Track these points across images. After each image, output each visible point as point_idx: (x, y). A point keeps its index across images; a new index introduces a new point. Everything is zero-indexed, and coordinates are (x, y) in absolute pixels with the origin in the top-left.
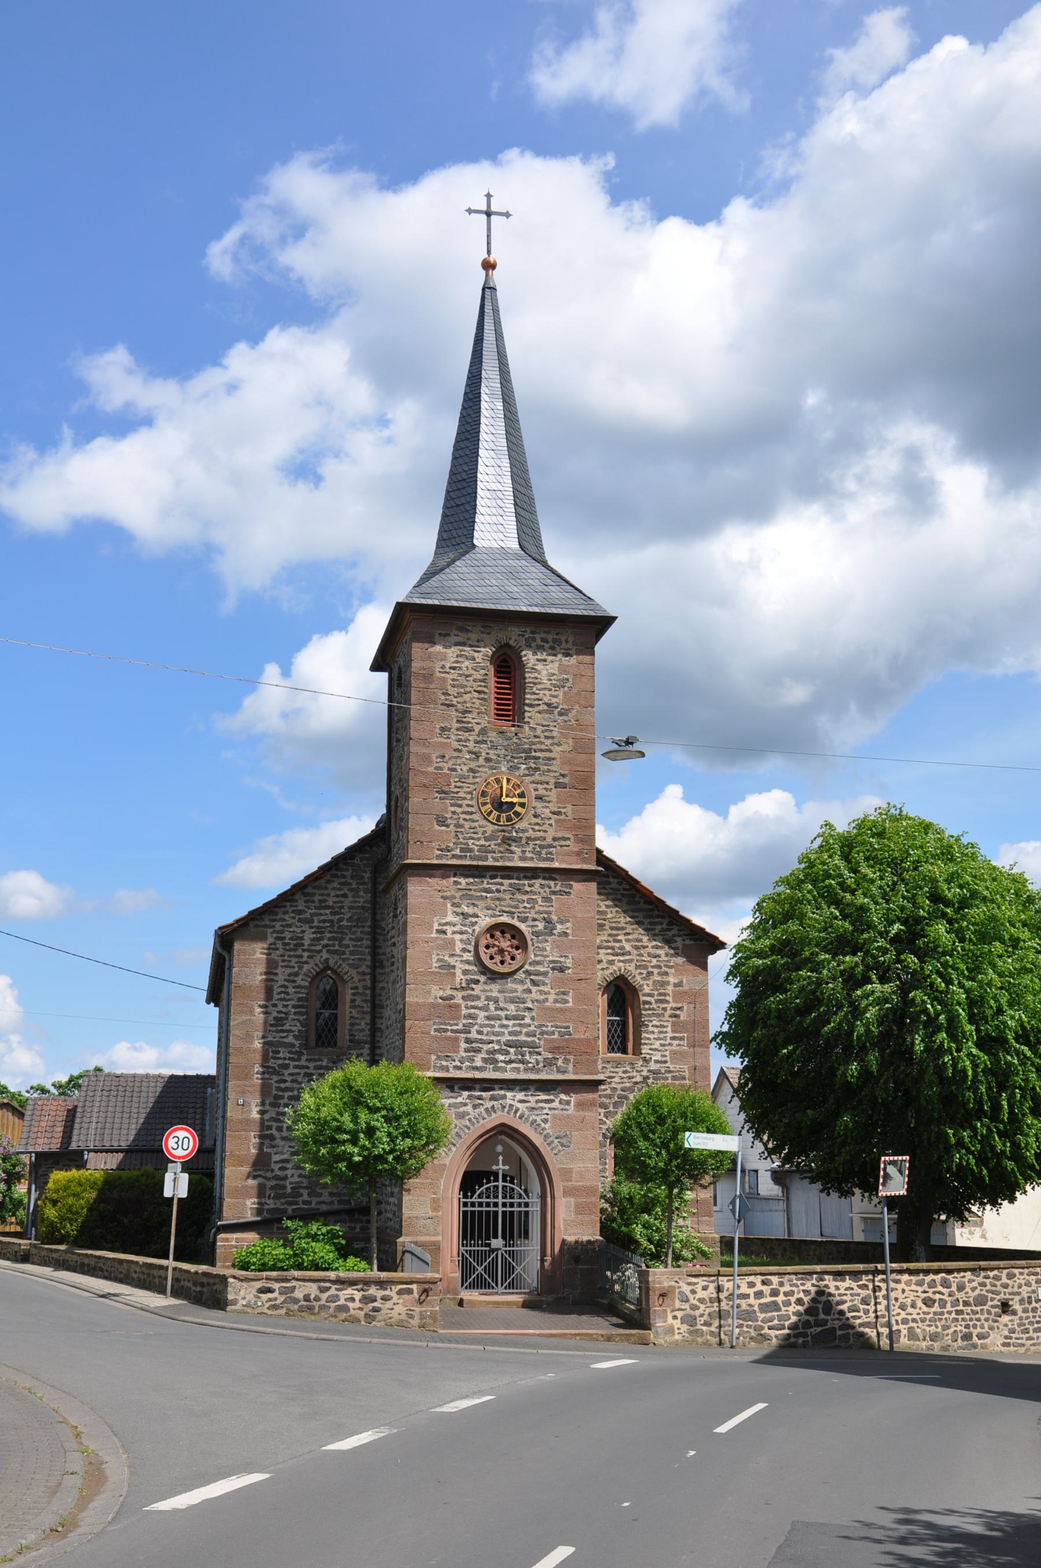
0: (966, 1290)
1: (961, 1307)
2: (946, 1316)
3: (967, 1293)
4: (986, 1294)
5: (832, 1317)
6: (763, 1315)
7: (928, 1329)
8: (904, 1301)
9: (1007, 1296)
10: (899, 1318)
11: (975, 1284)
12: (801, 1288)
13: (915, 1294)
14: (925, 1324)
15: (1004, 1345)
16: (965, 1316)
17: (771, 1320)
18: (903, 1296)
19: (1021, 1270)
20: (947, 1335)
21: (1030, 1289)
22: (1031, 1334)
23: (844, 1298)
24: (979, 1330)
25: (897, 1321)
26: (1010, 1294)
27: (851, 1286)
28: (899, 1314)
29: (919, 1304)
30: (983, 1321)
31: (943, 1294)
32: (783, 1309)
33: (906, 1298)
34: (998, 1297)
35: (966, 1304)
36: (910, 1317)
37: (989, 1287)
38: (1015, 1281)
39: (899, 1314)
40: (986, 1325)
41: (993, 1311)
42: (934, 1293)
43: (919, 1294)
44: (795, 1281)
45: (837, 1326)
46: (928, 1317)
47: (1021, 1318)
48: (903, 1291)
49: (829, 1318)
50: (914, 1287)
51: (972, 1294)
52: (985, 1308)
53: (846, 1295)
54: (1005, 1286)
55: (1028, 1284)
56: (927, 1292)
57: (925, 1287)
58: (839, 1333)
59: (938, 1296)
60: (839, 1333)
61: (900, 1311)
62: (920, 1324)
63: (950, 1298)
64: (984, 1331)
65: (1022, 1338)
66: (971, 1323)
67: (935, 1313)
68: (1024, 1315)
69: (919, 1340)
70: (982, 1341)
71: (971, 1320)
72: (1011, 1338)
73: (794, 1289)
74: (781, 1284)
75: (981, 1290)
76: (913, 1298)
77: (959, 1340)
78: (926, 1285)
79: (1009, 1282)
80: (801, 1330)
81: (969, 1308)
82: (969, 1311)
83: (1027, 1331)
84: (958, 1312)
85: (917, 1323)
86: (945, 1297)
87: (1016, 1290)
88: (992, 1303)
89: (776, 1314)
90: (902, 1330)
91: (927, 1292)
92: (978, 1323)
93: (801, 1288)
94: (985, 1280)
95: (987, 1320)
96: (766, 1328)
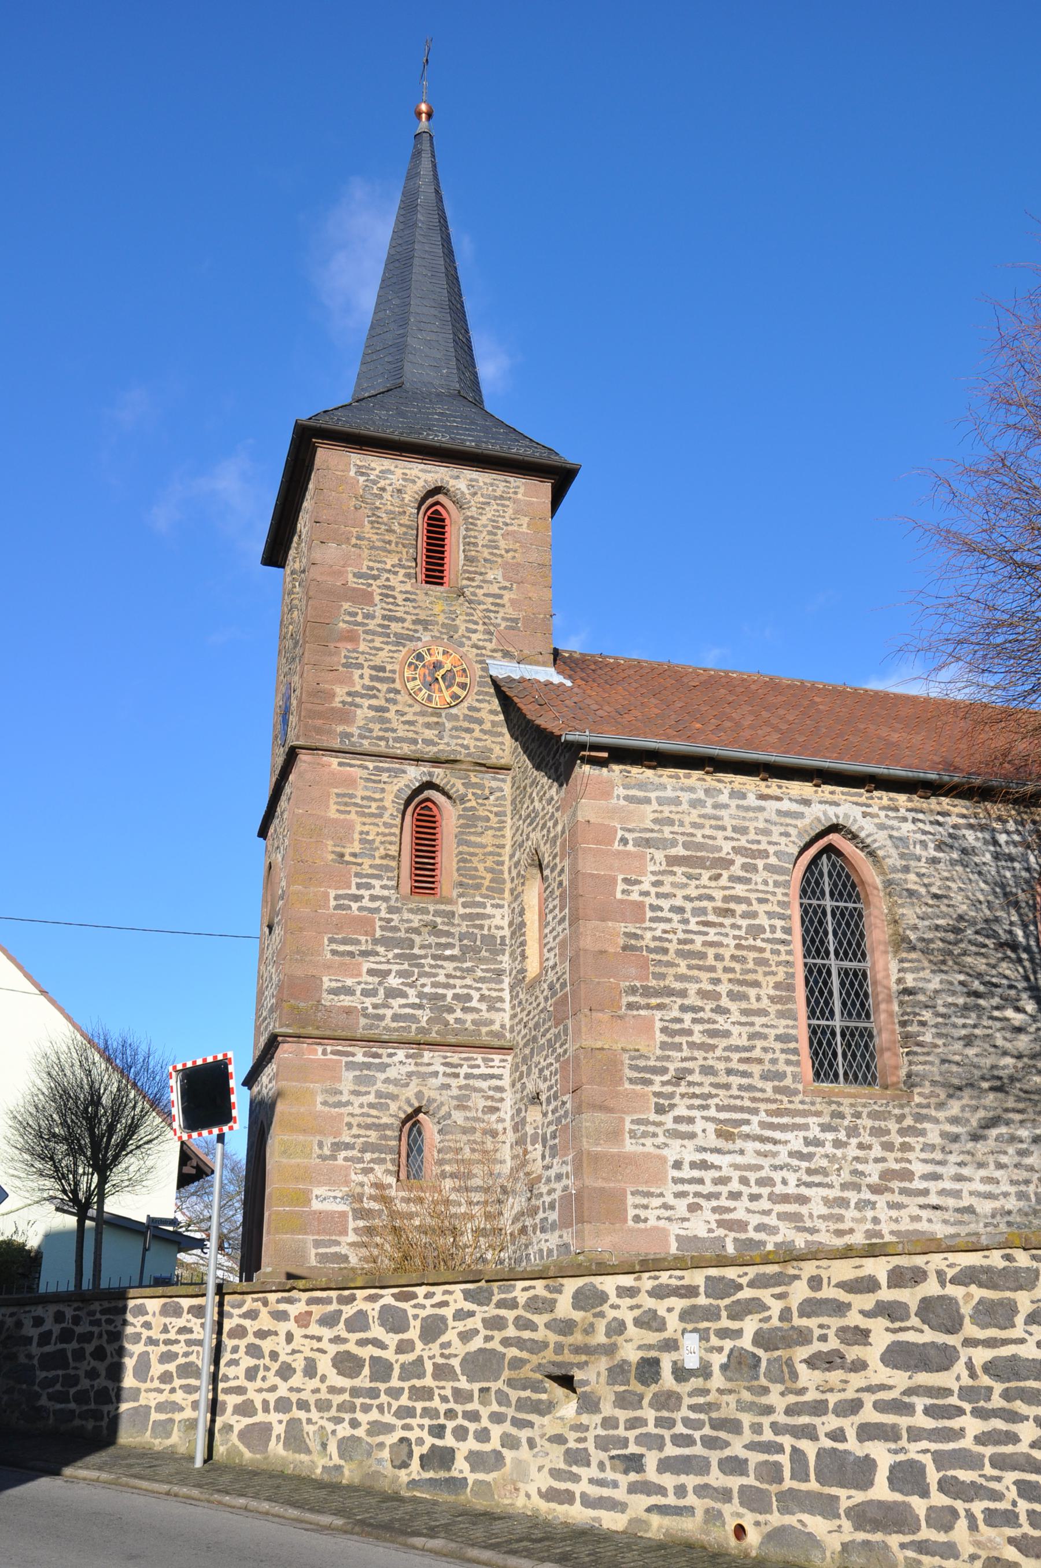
0: (444, 1339)
1: (428, 1381)
2: (384, 1398)
3: (447, 1345)
4: (501, 1349)
5: (148, 1385)
6: (44, 1374)
7: (330, 1426)
8: (289, 1359)
9: (568, 1357)
10: (272, 1397)
11: (470, 1323)
12: (105, 1327)
13: (316, 1345)
14: (326, 1415)
15: (551, 1495)
16: (436, 1403)
17: (54, 1381)
18: (289, 1349)
19: (627, 1281)
20: (381, 1445)
21: (652, 1337)
22: (651, 1474)
23: (174, 1348)
24: (471, 1444)
25: (266, 1403)
26: (577, 1350)
27: (189, 1325)
28: (273, 1389)
29: (325, 1365)
30: (485, 1422)
31: (382, 1346)
32: (72, 1364)
33: (294, 1352)
34: (535, 1359)
35: (442, 1372)
36: (294, 1397)
37: (511, 1332)
38: (601, 1315)
39: (273, 1389)
40: (496, 1432)
41: (514, 1395)
42: (362, 1343)
43: (324, 1345)
44: (98, 1316)
45: (153, 1404)
46: (337, 1399)
47: (609, 1423)
48: (289, 1338)
49: (143, 1386)
50: (314, 1329)
51: (459, 1349)
52: (494, 1386)
53: (177, 1342)
54: (566, 1327)
55: (650, 1321)
56: (345, 1341)
57: (340, 1330)
58: (155, 1416)
59: (367, 1352)
60: (155, 1416)
61: (278, 1381)
62: (314, 1415)
63: (403, 1358)
64: (486, 1447)
65: (615, 1485)
66: (450, 1425)
67: (355, 1392)
68: (622, 1415)
69: (308, 1451)
70: (481, 1476)
71: (450, 1414)
72: (576, 1478)
73: (96, 1330)
74: (76, 1320)
75: (488, 1339)
76: (310, 1354)
77: (415, 1463)
78: (342, 1325)
79: (578, 1315)
80: (93, 1406)
81: (449, 1385)
82: (448, 1392)
83: (634, 1463)
84: (426, 1394)
85: (308, 1411)
86: (389, 1355)
87: (600, 1337)
88: (514, 1374)
89: (60, 1372)
90: (275, 1425)
91: (345, 1341)
92: (472, 1427)
93: (105, 1327)
94: (502, 1312)
95: (497, 1418)
96: (44, 1397)
